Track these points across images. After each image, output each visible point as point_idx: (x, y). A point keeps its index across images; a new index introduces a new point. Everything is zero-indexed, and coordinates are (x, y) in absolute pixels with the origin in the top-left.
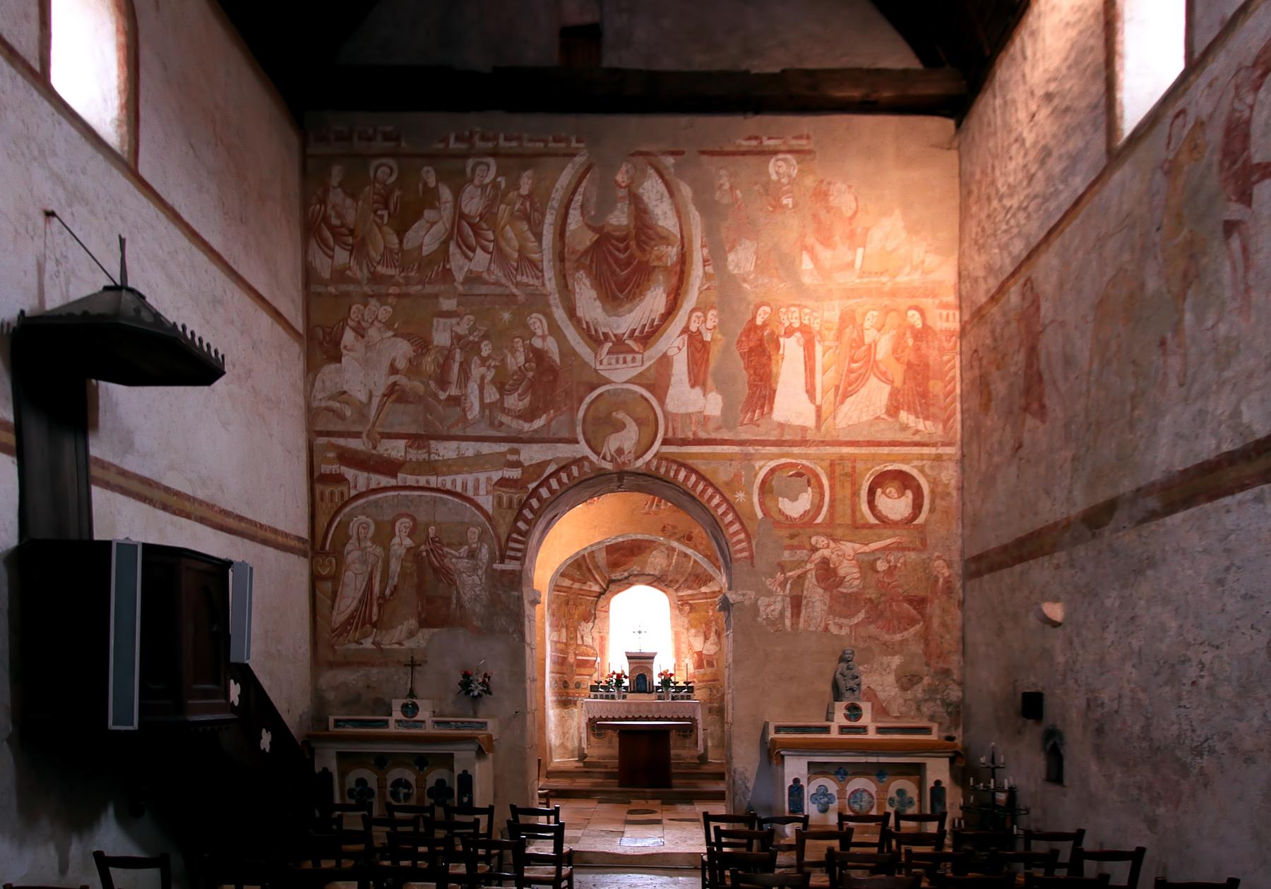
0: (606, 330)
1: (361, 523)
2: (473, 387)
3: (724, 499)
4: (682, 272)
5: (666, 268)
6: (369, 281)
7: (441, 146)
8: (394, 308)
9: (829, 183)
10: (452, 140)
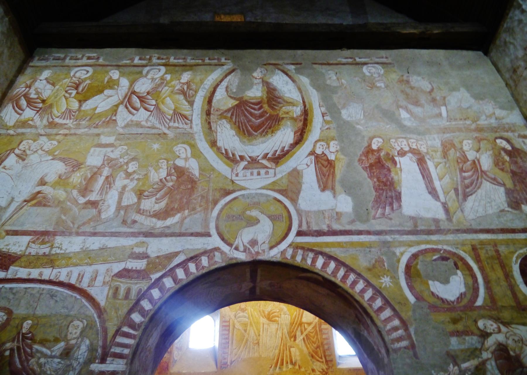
0: (240, 154)
3: (369, 284)
4: (305, 120)
5: (292, 118)
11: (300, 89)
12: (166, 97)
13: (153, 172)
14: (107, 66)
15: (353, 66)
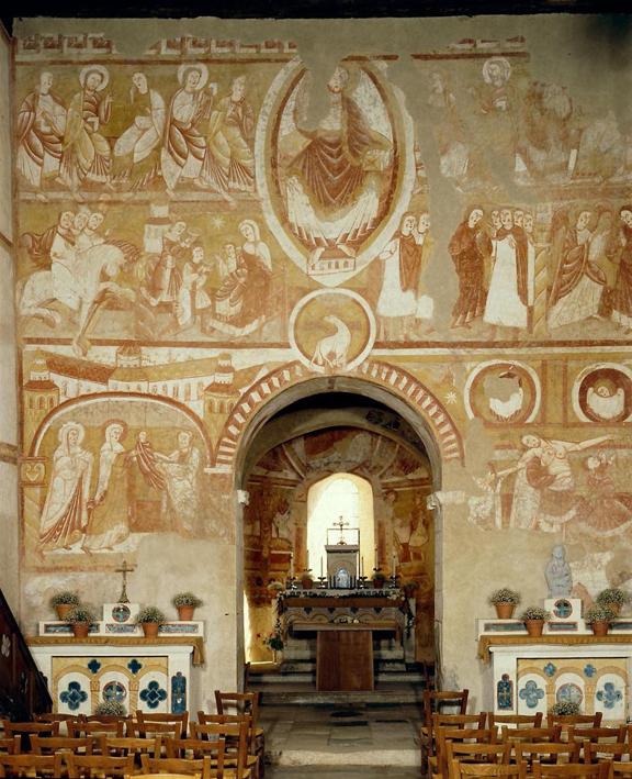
1: (71, 429)
2: (185, 293)
3: (436, 401)
4: (395, 176)
5: (378, 173)
6: (79, 187)
7: (153, 52)
8: (105, 215)
9: (543, 85)
10: (164, 47)
11: (391, 116)
12: (216, 132)
13: (221, 261)
14: (126, 62)
15: (471, 60)
